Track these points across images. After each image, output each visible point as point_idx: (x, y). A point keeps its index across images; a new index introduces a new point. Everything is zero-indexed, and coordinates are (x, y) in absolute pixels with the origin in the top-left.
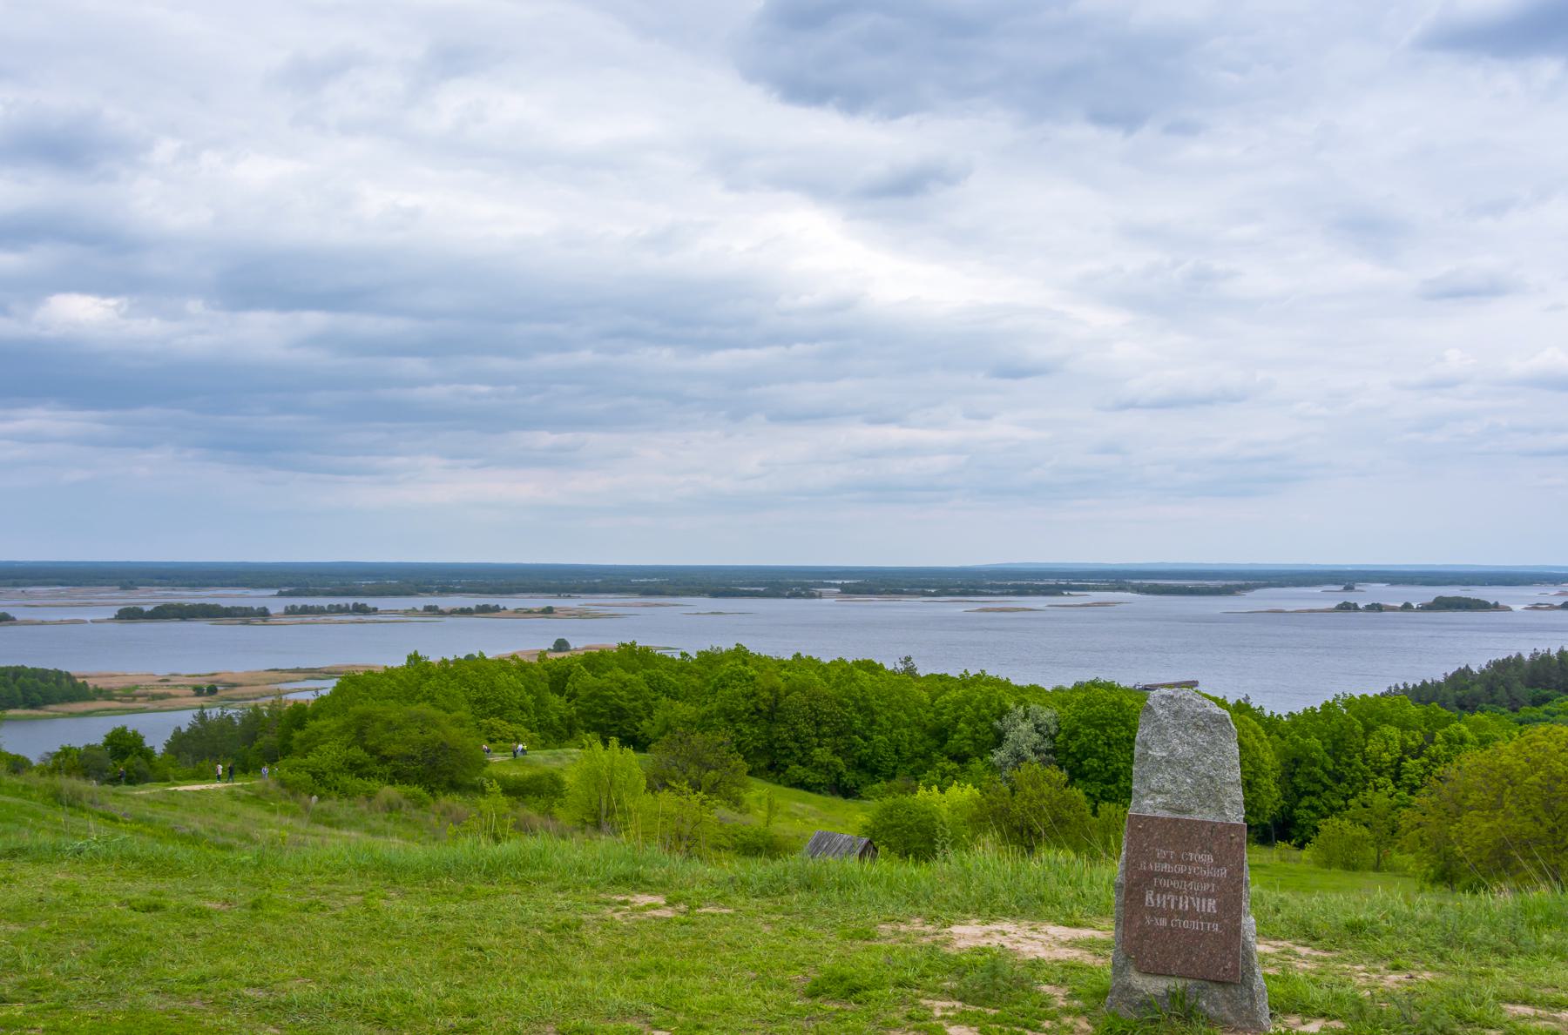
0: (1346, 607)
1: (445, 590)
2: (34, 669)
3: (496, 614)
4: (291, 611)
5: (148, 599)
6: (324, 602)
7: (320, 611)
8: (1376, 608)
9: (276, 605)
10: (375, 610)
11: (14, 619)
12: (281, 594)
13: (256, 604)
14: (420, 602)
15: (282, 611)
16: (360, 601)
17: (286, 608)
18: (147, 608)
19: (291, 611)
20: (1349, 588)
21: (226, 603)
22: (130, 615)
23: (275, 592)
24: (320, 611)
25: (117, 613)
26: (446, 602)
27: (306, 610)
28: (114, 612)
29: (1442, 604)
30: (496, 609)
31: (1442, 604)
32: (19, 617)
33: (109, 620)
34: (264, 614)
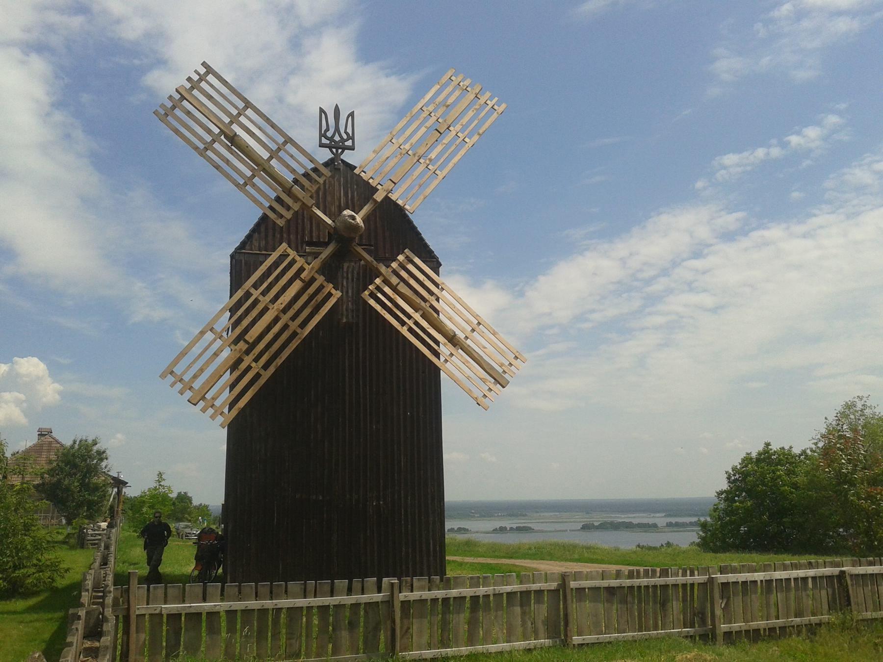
4: (670, 525)
5: (597, 519)
11: (533, 529)
13: (651, 521)
15: (665, 525)
17: (667, 523)
18: (596, 524)
21: (636, 521)
23: (663, 515)
24: (683, 525)
25: (581, 526)
27: (677, 525)
28: (579, 526)
32: (536, 528)
33: (579, 530)
34: (655, 526)
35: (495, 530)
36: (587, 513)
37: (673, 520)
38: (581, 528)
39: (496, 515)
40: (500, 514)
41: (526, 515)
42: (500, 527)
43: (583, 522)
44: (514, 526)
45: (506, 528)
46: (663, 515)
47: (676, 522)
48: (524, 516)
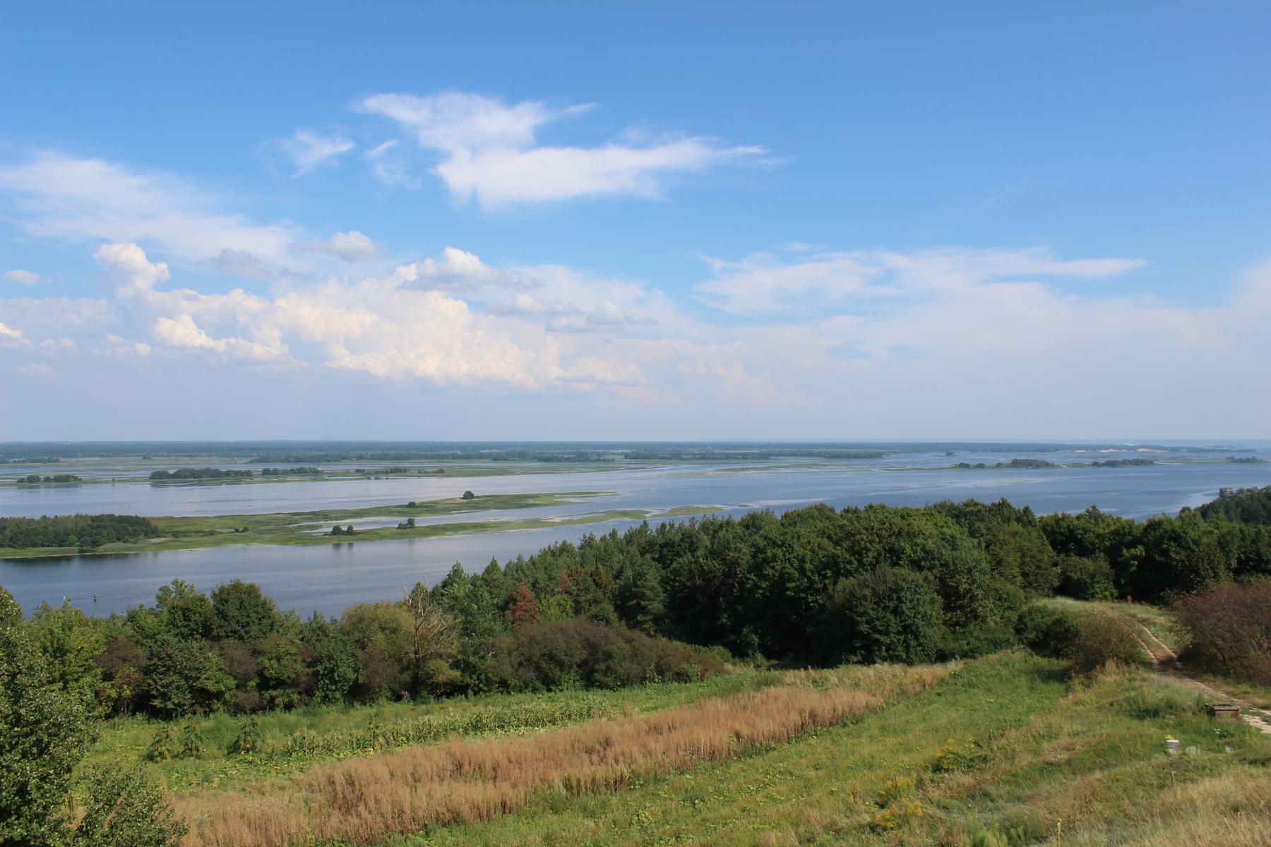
0: (964, 466)
1: (360, 458)
2: (121, 517)
3: (404, 474)
4: (266, 472)
6: (288, 467)
7: (285, 473)
8: (981, 466)
9: (260, 468)
10: (322, 471)
11: (81, 480)
12: (251, 462)
13: (243, 468)
14: (354, 466)
16: (312, 466)
18: (171, 472)
19: (266, 472)
20: (949, 454)
21: (224, 469)
22: (160, 479)
23: (248, 460)
24: (285, 473)
26: (367, 466)
27: (275, 473)
28: (148, 474)
29: (1015, 464)
30: (405, 470)
31: (1015, 464)
34: (249, 474)
35: (22, 481)
36: (144, 458)
37: (271, 467)
38: (151, 478)
39: (11, 461)
40: (16, 460)
41: (58, 461)
42: (28, 478)
43: (153, 469)
44: (52, 475)
45: (38, 479)
46: (248, 460)
47: (275, 469)
48: (54, 461)
